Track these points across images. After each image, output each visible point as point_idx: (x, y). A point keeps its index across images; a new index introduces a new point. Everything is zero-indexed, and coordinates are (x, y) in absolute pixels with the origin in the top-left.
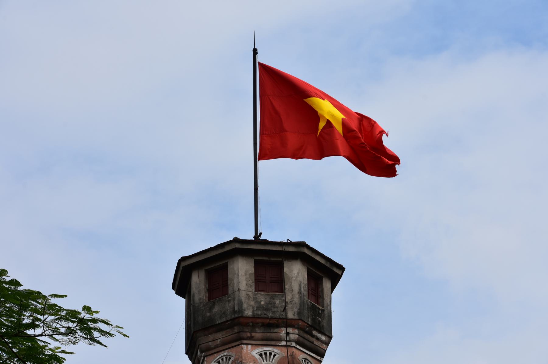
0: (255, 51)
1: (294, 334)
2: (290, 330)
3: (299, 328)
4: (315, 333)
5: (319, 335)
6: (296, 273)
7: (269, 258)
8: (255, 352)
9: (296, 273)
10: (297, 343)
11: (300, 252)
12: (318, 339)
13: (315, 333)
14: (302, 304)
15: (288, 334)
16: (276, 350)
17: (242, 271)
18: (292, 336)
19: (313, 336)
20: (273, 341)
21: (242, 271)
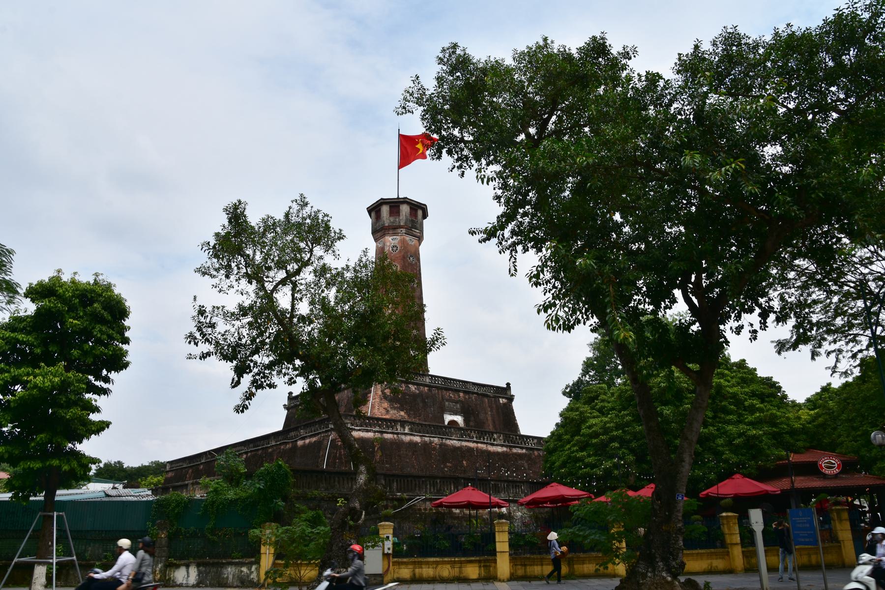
1: (404, 231)
6: (405, 209)
7: (394, 205)
8: (390, 239)
9: (405, 209)
11: (406, 201)
14: (407, 219)
17: (385, 210)
21: (385, 210)
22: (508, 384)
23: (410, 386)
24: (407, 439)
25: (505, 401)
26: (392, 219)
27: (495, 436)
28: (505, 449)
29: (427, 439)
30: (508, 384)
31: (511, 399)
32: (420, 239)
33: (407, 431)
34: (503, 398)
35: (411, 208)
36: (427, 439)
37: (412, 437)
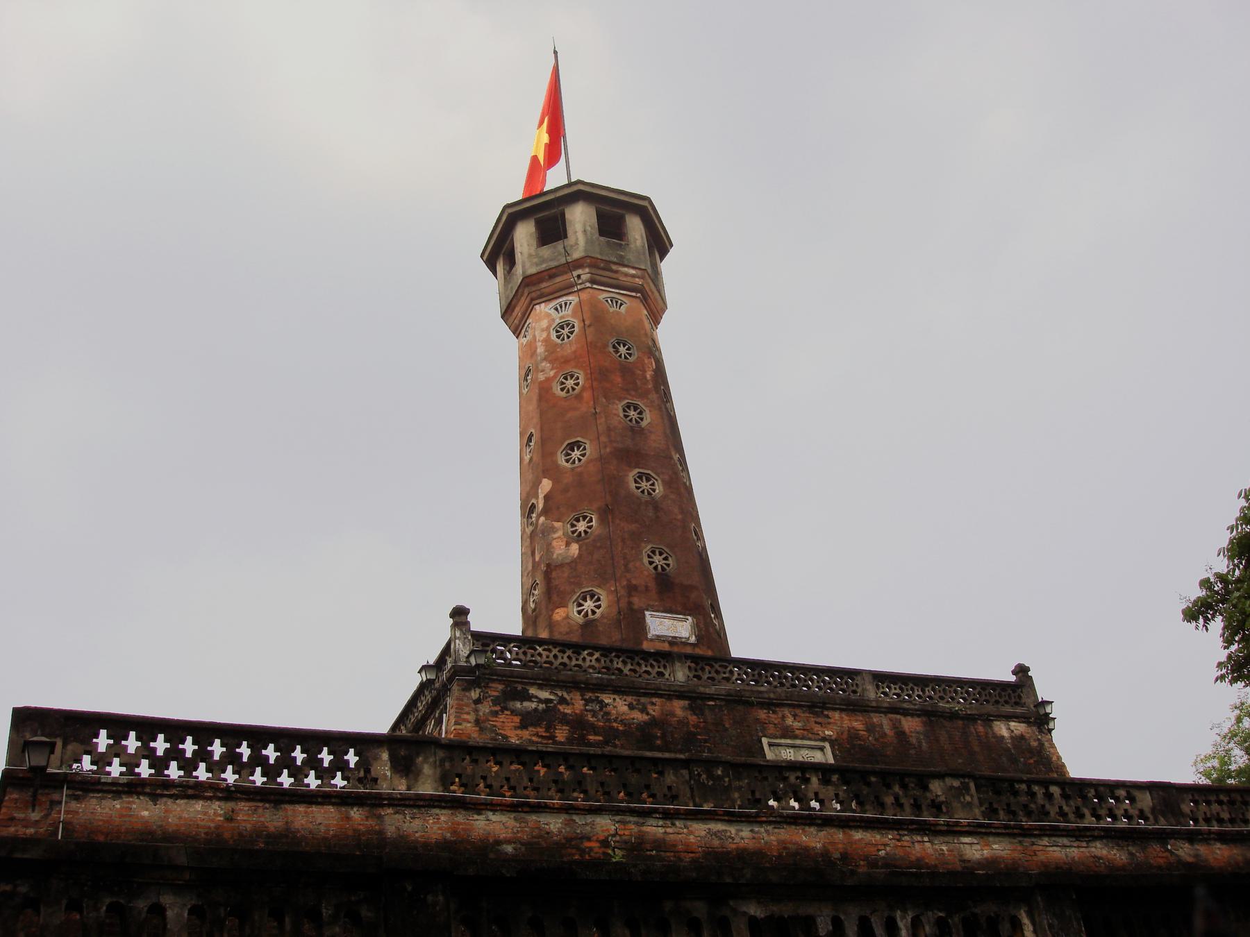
0: (555, 52)
1: (585, 274)
2: (580, 272)
3: (590, 266)
4: (614, 267)
5: (626, 269)
9: (580, 218)
10: (593, 281)
11: (579, 193)
12: (626, 275)
13: (614, 267)
14: (589, 242)
15: (579, 276)
16: (570, 298)
17: (524, 235)
18: (584, 277)
19: (616, 272)
20: (567, 289)
22: (1022, 671)
23: (607, 699)
24: (433, 826)
25: (1018, 727)
26: (546, 251)
27: (936, 787)
28: (999, 848)
29: (554, 824)
30: (1022, 671)
31: (1041, 719)
32: (656, 311)
33: (427, 788)
34: (1008, 717)
35: (601, 216)
36: (554, 824)
37: (460, 817)
